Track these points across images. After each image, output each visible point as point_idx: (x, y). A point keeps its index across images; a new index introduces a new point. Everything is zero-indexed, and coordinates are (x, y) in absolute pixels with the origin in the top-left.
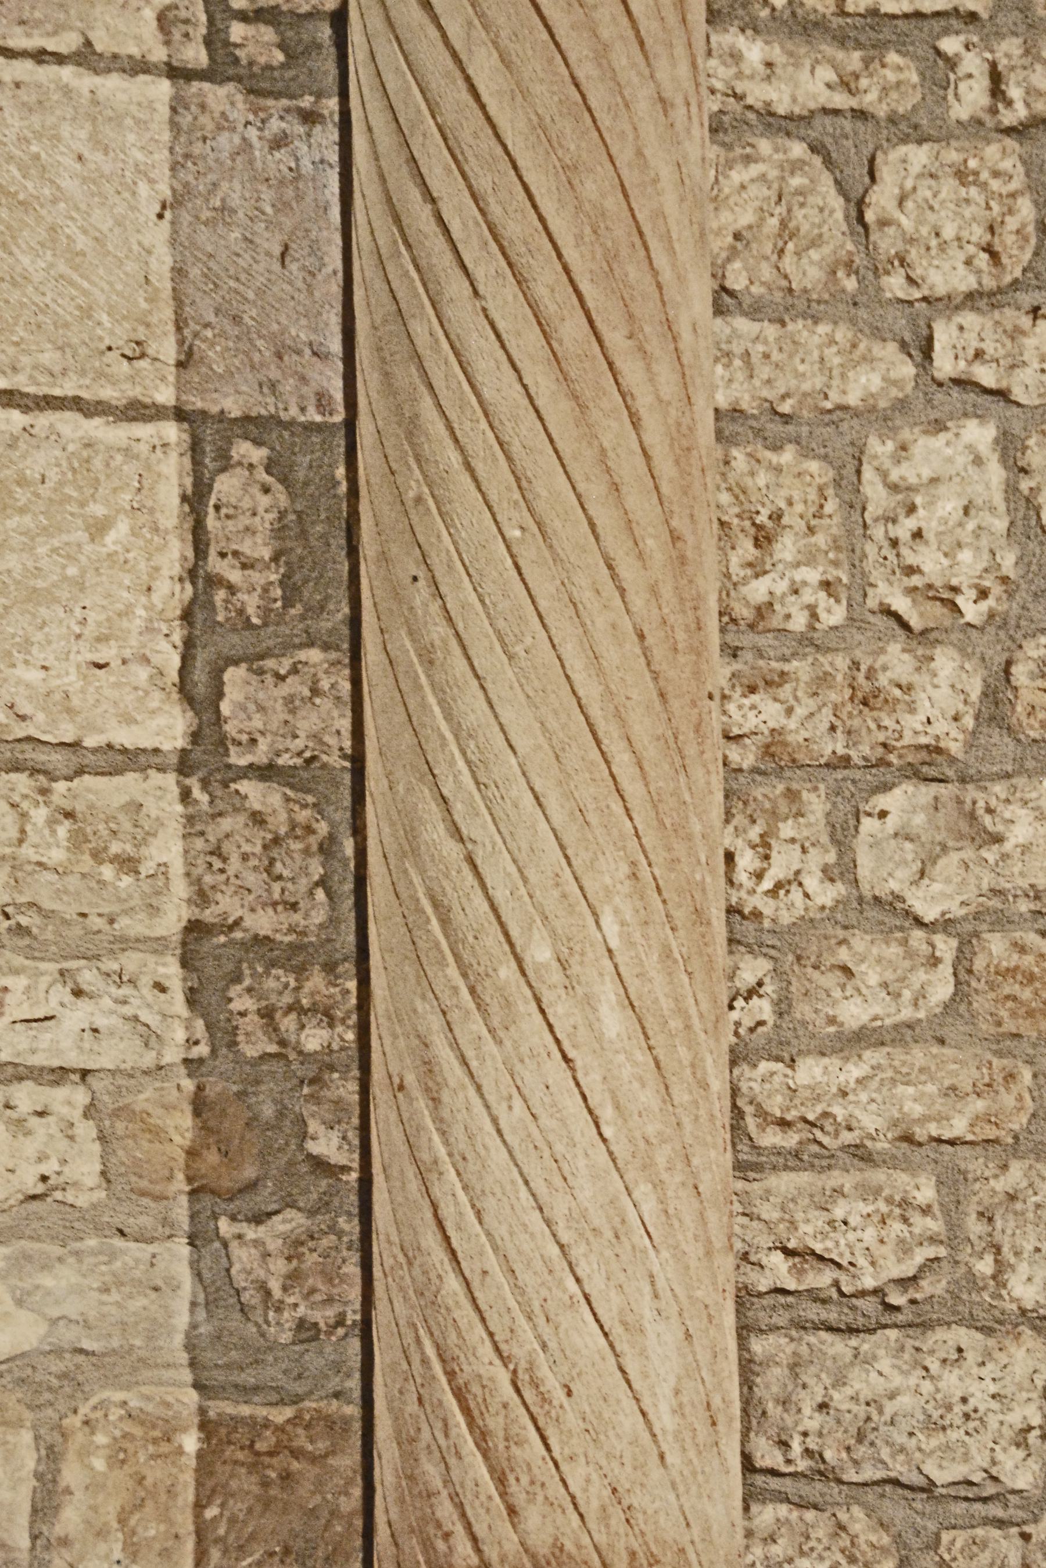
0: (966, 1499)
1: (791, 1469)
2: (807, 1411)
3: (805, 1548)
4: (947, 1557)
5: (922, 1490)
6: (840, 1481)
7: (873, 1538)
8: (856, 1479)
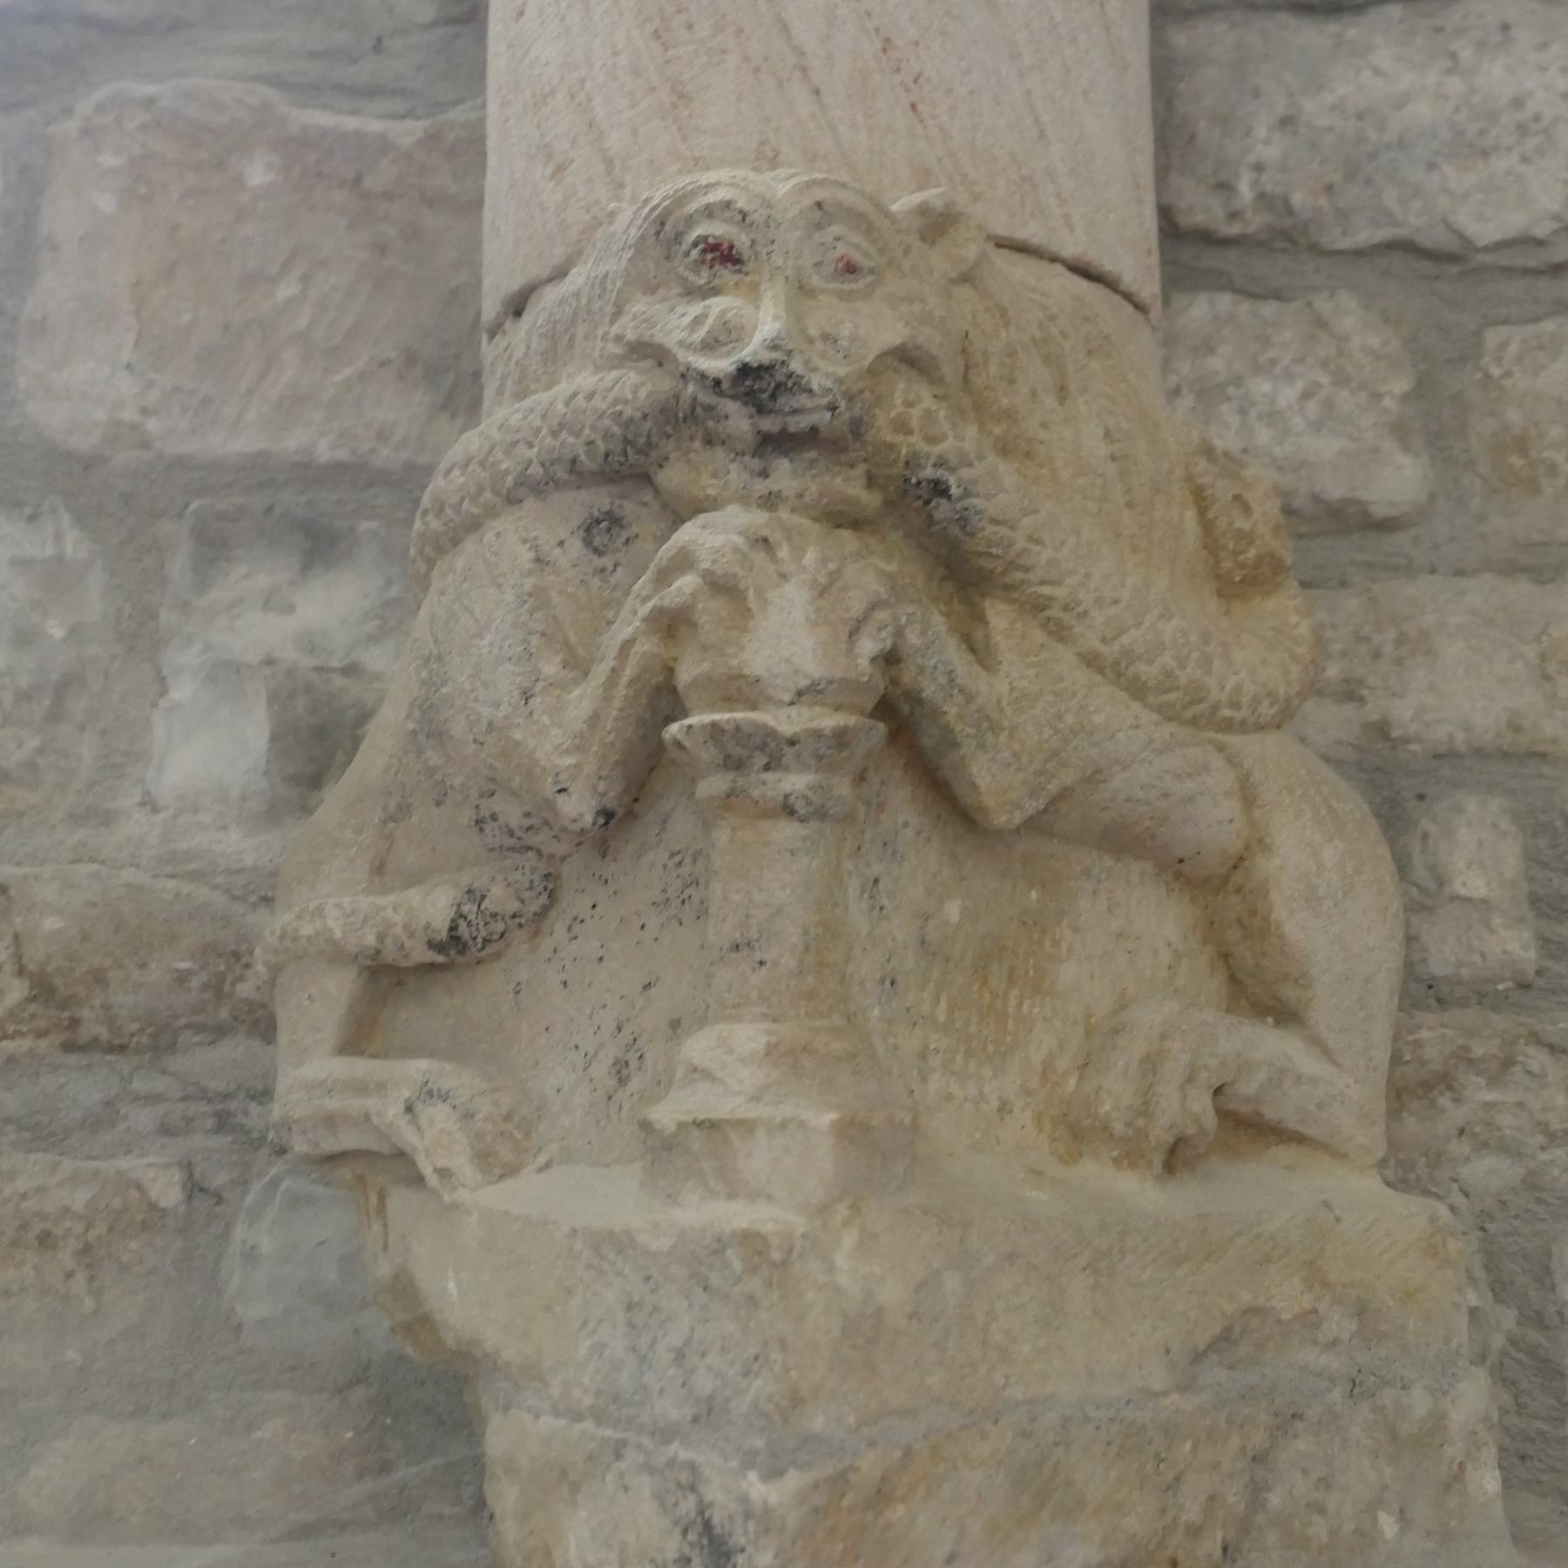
0: (1526, 272)
1: (1235, 229)
2: (1261, 132)
3: (1263, 359)
4: (1495, 371)
5: (1453, 258)
6: (1318, 251)
7: (1374, 341)
8: (1345, 243)
